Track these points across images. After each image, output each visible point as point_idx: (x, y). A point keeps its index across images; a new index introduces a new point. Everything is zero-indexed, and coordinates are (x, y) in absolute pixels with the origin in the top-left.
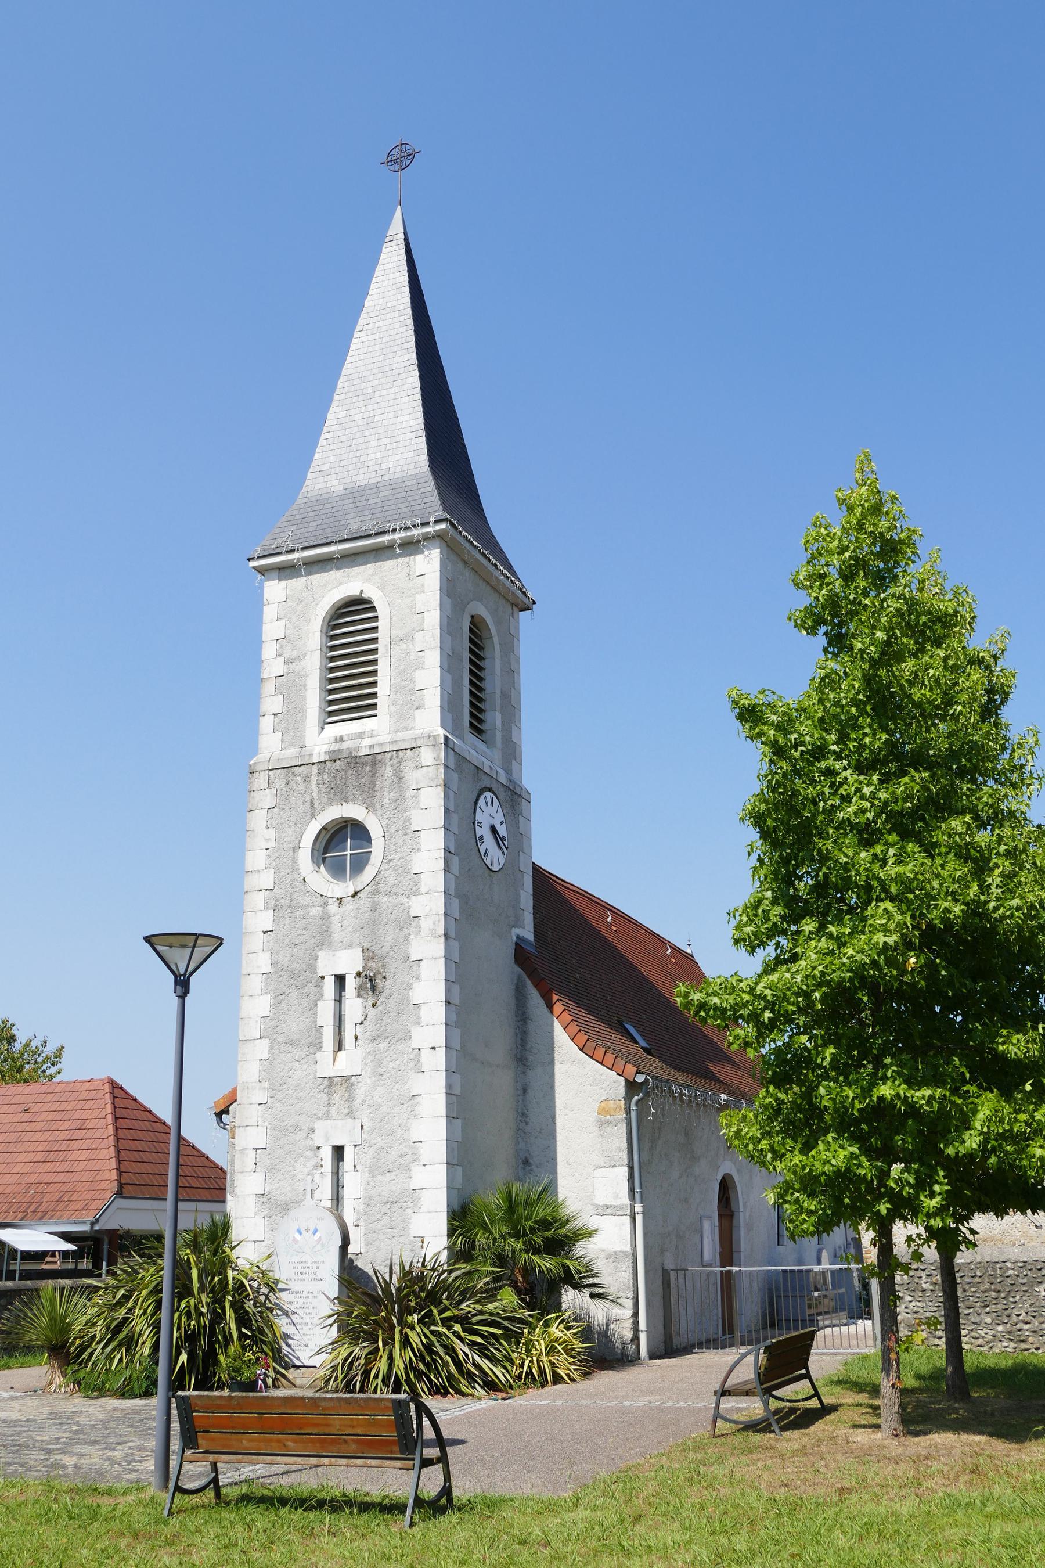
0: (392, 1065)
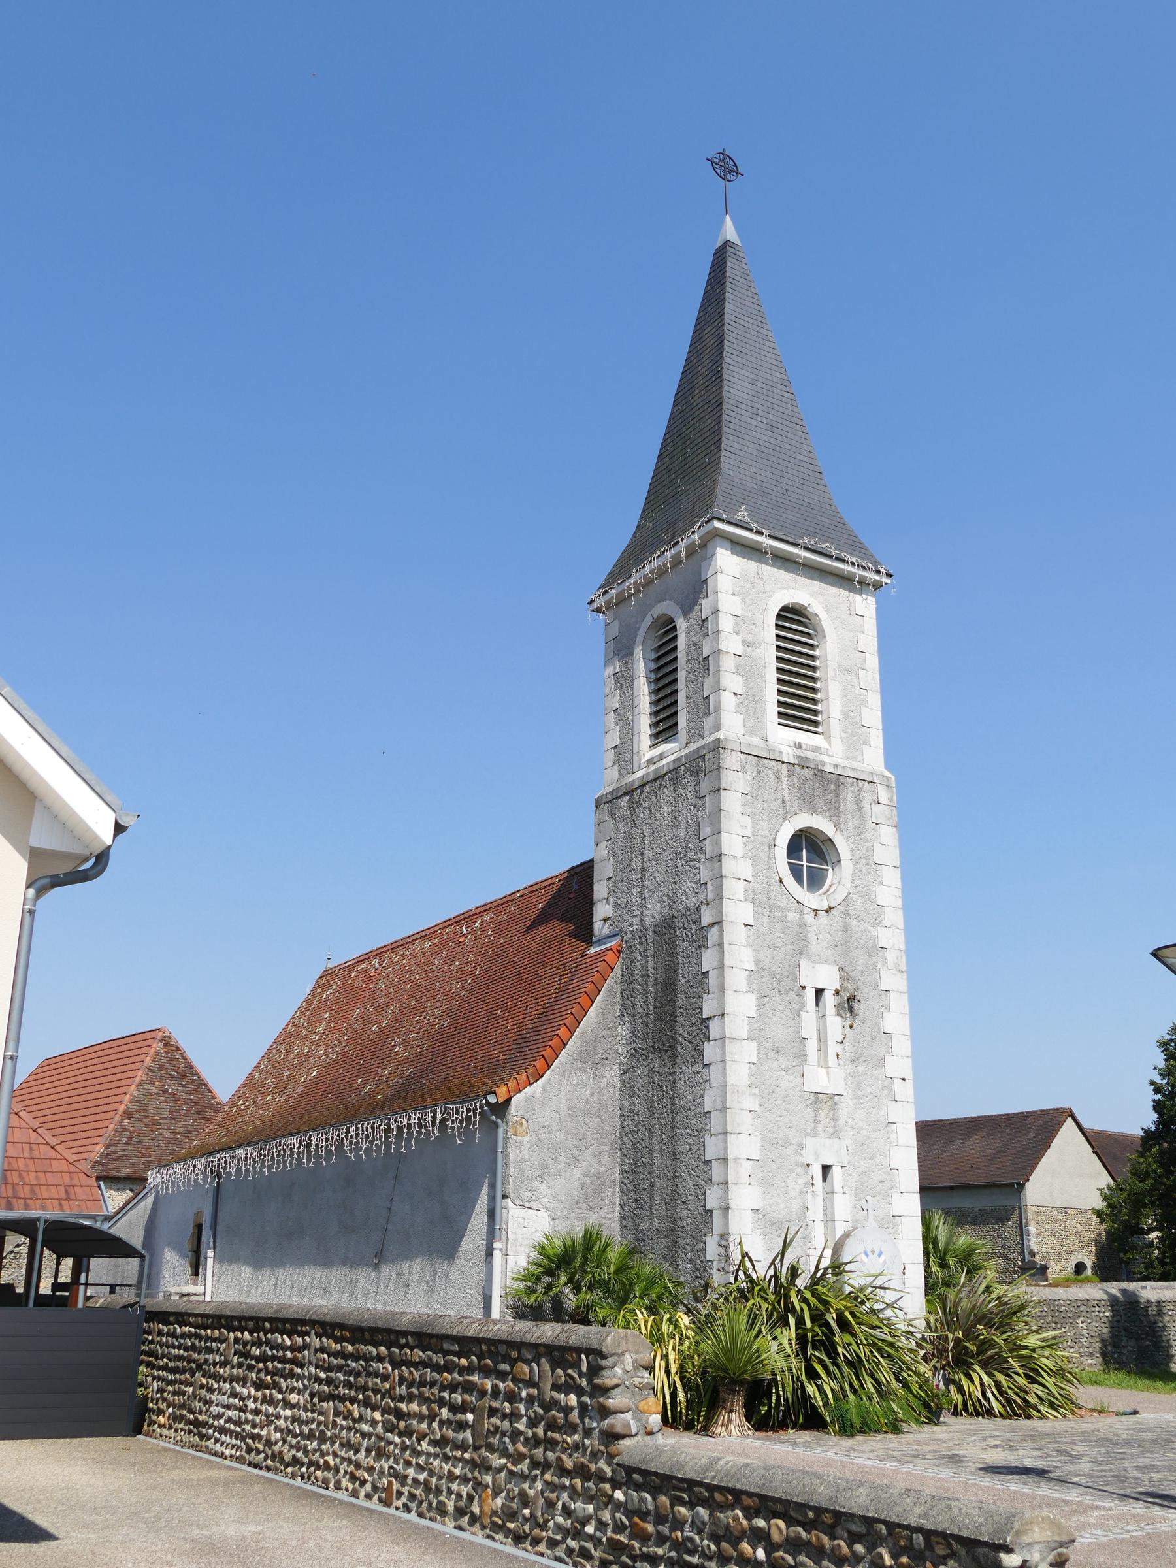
0: (869, 1090)
